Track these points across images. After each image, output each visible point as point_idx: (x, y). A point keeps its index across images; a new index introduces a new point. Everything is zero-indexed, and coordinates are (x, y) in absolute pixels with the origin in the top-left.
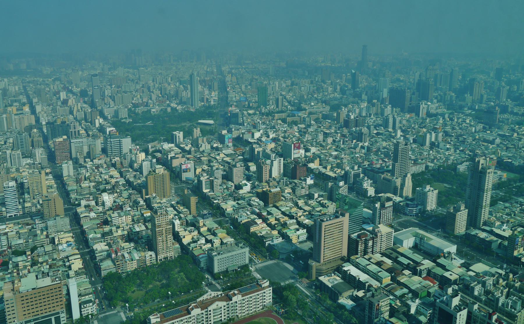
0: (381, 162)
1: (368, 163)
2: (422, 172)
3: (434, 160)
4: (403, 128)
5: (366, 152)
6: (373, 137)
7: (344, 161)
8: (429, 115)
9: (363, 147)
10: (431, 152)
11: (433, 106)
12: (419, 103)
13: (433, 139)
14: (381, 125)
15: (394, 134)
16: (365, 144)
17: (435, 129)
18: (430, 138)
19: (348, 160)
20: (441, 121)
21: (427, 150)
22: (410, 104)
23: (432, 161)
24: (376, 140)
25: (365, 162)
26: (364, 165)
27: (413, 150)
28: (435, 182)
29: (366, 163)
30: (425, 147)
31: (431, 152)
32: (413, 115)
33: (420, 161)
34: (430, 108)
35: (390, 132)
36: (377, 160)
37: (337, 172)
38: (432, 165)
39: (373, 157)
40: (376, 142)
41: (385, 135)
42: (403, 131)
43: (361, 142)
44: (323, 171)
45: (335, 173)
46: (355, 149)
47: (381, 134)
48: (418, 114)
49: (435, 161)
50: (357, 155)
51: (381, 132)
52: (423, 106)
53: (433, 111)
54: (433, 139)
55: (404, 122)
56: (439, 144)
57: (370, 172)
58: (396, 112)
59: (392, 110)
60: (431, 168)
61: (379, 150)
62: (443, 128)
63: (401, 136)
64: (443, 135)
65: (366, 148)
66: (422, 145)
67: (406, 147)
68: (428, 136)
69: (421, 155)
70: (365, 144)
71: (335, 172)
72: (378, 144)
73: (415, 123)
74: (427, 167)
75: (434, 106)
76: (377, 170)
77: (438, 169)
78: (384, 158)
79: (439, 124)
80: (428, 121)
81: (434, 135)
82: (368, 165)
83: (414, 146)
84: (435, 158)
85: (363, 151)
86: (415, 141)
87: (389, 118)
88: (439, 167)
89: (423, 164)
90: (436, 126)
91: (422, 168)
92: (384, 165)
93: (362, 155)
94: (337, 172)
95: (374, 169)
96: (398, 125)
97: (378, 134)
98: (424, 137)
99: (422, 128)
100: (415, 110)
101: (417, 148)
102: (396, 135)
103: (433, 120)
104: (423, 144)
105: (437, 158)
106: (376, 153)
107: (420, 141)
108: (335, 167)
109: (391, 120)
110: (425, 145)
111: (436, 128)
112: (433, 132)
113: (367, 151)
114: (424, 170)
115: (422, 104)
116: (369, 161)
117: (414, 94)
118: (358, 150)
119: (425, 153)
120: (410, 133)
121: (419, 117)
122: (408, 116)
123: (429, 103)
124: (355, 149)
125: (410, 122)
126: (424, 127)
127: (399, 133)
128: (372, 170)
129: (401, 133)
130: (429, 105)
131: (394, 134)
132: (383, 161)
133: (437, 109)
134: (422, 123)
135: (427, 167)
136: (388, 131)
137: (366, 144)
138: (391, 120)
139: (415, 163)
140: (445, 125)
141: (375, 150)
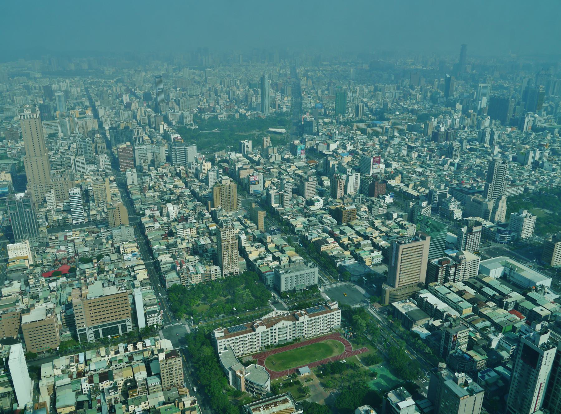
0: (473, 182)
1: (457, 182)
2: (520, 195)
3: (535, 181)
4: (502, 144)
5: (455, 169)
6: (466, 152)
7: (429, 179)
8: (535, 129)
9: (452, 164)
10: (533, 172)
11: (541, 119)
12: (524, 115)
13: (537, 158)
14: (476, 140)
15: (490, 151)
16: (455, 161)
17: (540, 146)
18: (534, 156)
19: (434, 178)
20: (549, 137)
21: (528, 170)
22: (513, 116)
23: (533, 183)
24: (468, 156)
25: (454, 181)
26: (452, 185)
27: (511, 170)
28: (534, 206)
29: (455, 182)
30: (526, 167)
31: (533, 172)
32: (516, 128)
33: (518, 182)
34: (537, 121)
35: (486, 148)
36: (468, 179)
37: (420, 191)
38: (533, 187)
39: (463, 175)
40: (469, 158)
41: (480, 151)
42: (501, 147)
43: (451, 158)
44: (405, 189)
45: (418, 191)
46: (443, 166)
47: (475, 150)
48: (521, 128)
49: (537, 183)
50: (444, 173)
51: (475, 147)
52: (529, 119)
53: (540, 125)
54: (537, 158)
55: (504, 137)
56: (543, 163)
57: (458, 192)
58: (495, 125)
59: (491, 122)
60: (531, 191)
61: (471, 167)
62: (550, 146)
63: (499, 152)
64: (549, 153)
65: (456, 165)
66: (523, 164)
67: (503, 165)
68: (531, 153)
69: (520, 176)
70: (455, 161)
71: (419, 190)
72: (471, 161)
73: (517, 139)
74: (526, 190)
75: (542, 119)
76: (467, 190)
77: (540, 193)
78: (476, 177)
79: (546, 141)
80: (532, 136)
81: (538, 152)
82: (457, 184)
83: (513, 165)
84: (537, 179)
85: (453, 168)
86: (514, 159)
87: (486, 132)
88: (541, 190)
89: (522, 185)
90: (542, 143)
91: (520, 190)
92: (475, 185)
93: (450, 172)
94: (420, 191)
95: (464, 189)
96: (496, 140)
97: (471, 150)
98: (527, 155)
99: (525, 144)
100: (518, 123)
101: (517, 167)
102: (493, 152)
103: (539, 135)
104: (524, 163)
105: (539, 180)
106: (467, 171)
107: (521, 159)
108: (418, 185)
109: (488, 134)
110: (527, 164)
111: (542, 145)
112: (538, 150)
113: (457, 169)
114: (522, 192)
115: (528, 116)
116: (458, 180)
117: (518, 104)
118: (446, 167)
119: (526, 174)
120: (510, 149)
121: (522, 131)
122: (510, 130)
123: (537, 116)
124: (443, 166)
125: (511, 137)
126: (528, 143)
127: (497, 149)
128: (461, 191)
129: (499, 150)
130: (535, 118)
131: (490, 151)
132: (475, 180)
133: (545, 122)
134: (525, 138)
135: (526, 190)
136: (484, 147)
137: (457, 161)
138: (488, 134)
139: (513, 184)
140: (553, 141)
141: (467, 167)
